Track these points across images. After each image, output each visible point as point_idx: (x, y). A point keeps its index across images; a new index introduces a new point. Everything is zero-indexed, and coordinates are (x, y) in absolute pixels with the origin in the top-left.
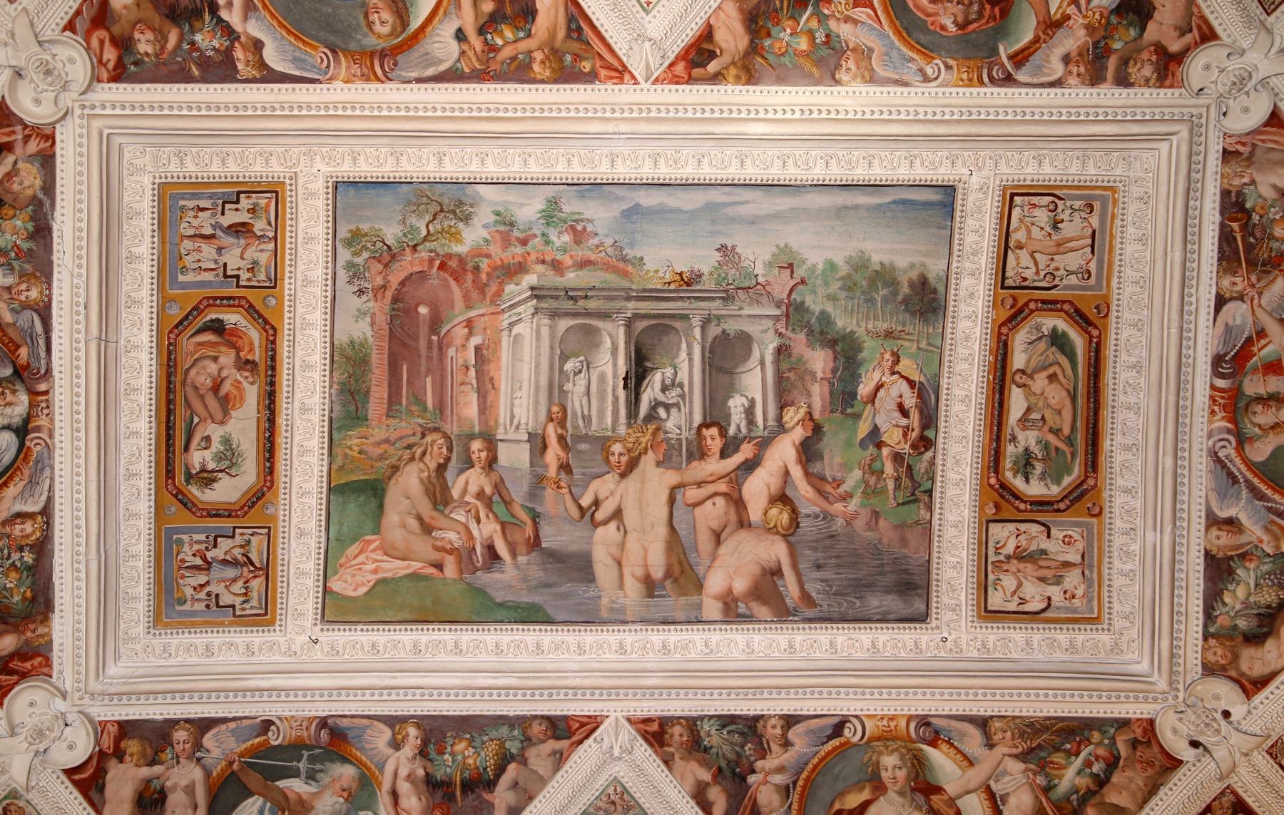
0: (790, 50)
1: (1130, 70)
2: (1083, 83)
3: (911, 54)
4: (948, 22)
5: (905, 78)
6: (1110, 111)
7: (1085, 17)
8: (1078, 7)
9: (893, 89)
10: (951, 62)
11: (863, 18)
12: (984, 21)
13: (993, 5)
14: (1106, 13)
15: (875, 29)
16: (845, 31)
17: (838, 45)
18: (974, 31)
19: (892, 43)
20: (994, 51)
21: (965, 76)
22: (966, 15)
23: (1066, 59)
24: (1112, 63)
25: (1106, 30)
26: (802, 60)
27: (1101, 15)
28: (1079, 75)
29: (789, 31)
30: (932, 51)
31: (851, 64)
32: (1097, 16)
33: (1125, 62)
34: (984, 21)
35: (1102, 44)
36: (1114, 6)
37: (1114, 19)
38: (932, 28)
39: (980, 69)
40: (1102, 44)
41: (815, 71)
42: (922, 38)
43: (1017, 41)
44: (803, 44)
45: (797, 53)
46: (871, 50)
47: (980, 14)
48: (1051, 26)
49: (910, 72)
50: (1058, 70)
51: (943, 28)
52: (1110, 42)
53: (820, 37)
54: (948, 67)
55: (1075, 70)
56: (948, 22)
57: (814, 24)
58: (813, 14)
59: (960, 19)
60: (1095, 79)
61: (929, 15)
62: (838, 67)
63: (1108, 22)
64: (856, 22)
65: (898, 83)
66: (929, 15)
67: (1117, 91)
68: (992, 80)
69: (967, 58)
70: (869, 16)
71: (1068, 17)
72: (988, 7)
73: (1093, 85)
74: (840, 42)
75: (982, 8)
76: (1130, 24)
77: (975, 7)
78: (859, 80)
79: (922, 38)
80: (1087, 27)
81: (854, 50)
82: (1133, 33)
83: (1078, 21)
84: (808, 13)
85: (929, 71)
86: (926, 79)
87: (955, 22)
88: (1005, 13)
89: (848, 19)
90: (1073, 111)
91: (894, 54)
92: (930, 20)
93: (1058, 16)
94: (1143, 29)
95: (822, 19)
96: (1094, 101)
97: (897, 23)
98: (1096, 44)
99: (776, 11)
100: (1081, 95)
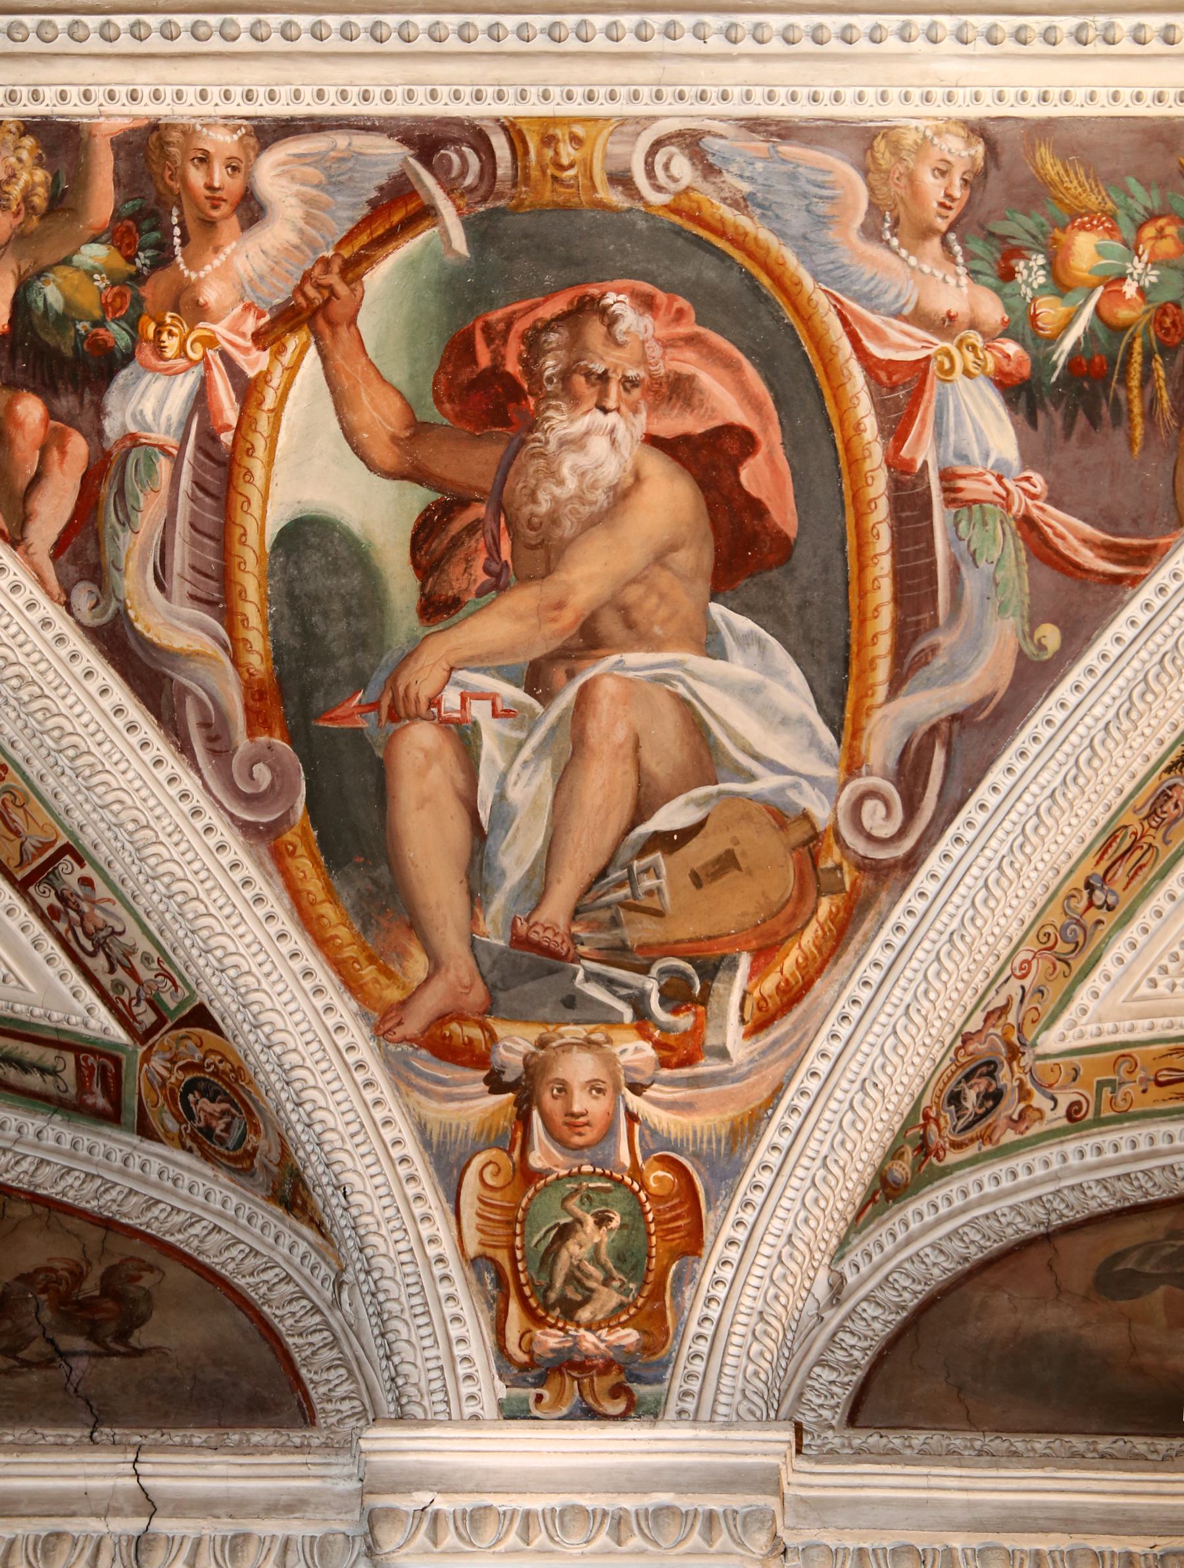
0: (1127, 231)
1: (40, 175)
2: (188, 133)
3: (744, 221)
4: (631, 320)
5: (758, 145)
6: (95, 44)
7: (210, 341)
8: (234, 371)
9: (802, 110)
10: (615, 197)
11: (895, 330)
12: (520, 326)
13: (497, 373)
14: (146, 353)
15: (857, 298)
16: (956, 292)
17: (977, 247)
18: (550, 294)
19: (801, 253)
20: (481, 231)
21: (567, 152)
22: (576, 341)
23: (251, 209)
24: (103, 199)
25: (138, 301)
26: (1093, 201)
27: (159, 350)
28: (205, 159)
29: (1130, 289)
30: (679, 232)
31: (933, 187)
32: (171, 344)
33: (63, 201)
34: (520, 326)
35: (142, 259)
36: (123, 376)
37: (117, 334)
38: (682, 302)
39: (521, 174)
40: (142, 259)
41: (1052, 167)
42: (711, 273)
43: (412, 265)
44: (1086, 250)
45: (1107, 222)
46: (871, 232)
47: (534, 344)
48: (308, 312)
49: (746, 164)
50: (272, 173)
51: (647, 304)
52: (119, 262)
53: (1032, 272)
54: (622, 179)
55: (220, 176)
56: (630, 319)
57: (1049, 311)
58: (1053, 340)
59: (595, 331)
60: (149, 150)
61: (691, 340)
62: (976, 181)
63: (134, 325)
64: (920, 318)
65: (782, 131)
66: (691, 340)
67: (74, 108)
68: (478, 138)
69: (564, 209)
70: (878, 335)
71: (259, 338)
72: (513, 367)
73: (155, 127)
74: (969, 256)
75: (530, 363)
76: (64, 320)
77: (550, 365)
78: (910, 139)
79: (711, 273)
80: (199, 312)
81: (926, 232)
82: (52, 294)
83: (231, 328)
84: (1068, 344)
85: (683, 168)
86: (691, 142)
87: (611, 320)
88: (459, 349)
89: (945, 325)
90: (216, 44)
91: (797, 221)
92: (684, 329)
93: (293, 343)
94: (20, 305)
95: (1024, 326)
96: (144, 76)
97: (790, 316)
98: (163, 258)
99: (1167, 350)
100: (191, 93)
